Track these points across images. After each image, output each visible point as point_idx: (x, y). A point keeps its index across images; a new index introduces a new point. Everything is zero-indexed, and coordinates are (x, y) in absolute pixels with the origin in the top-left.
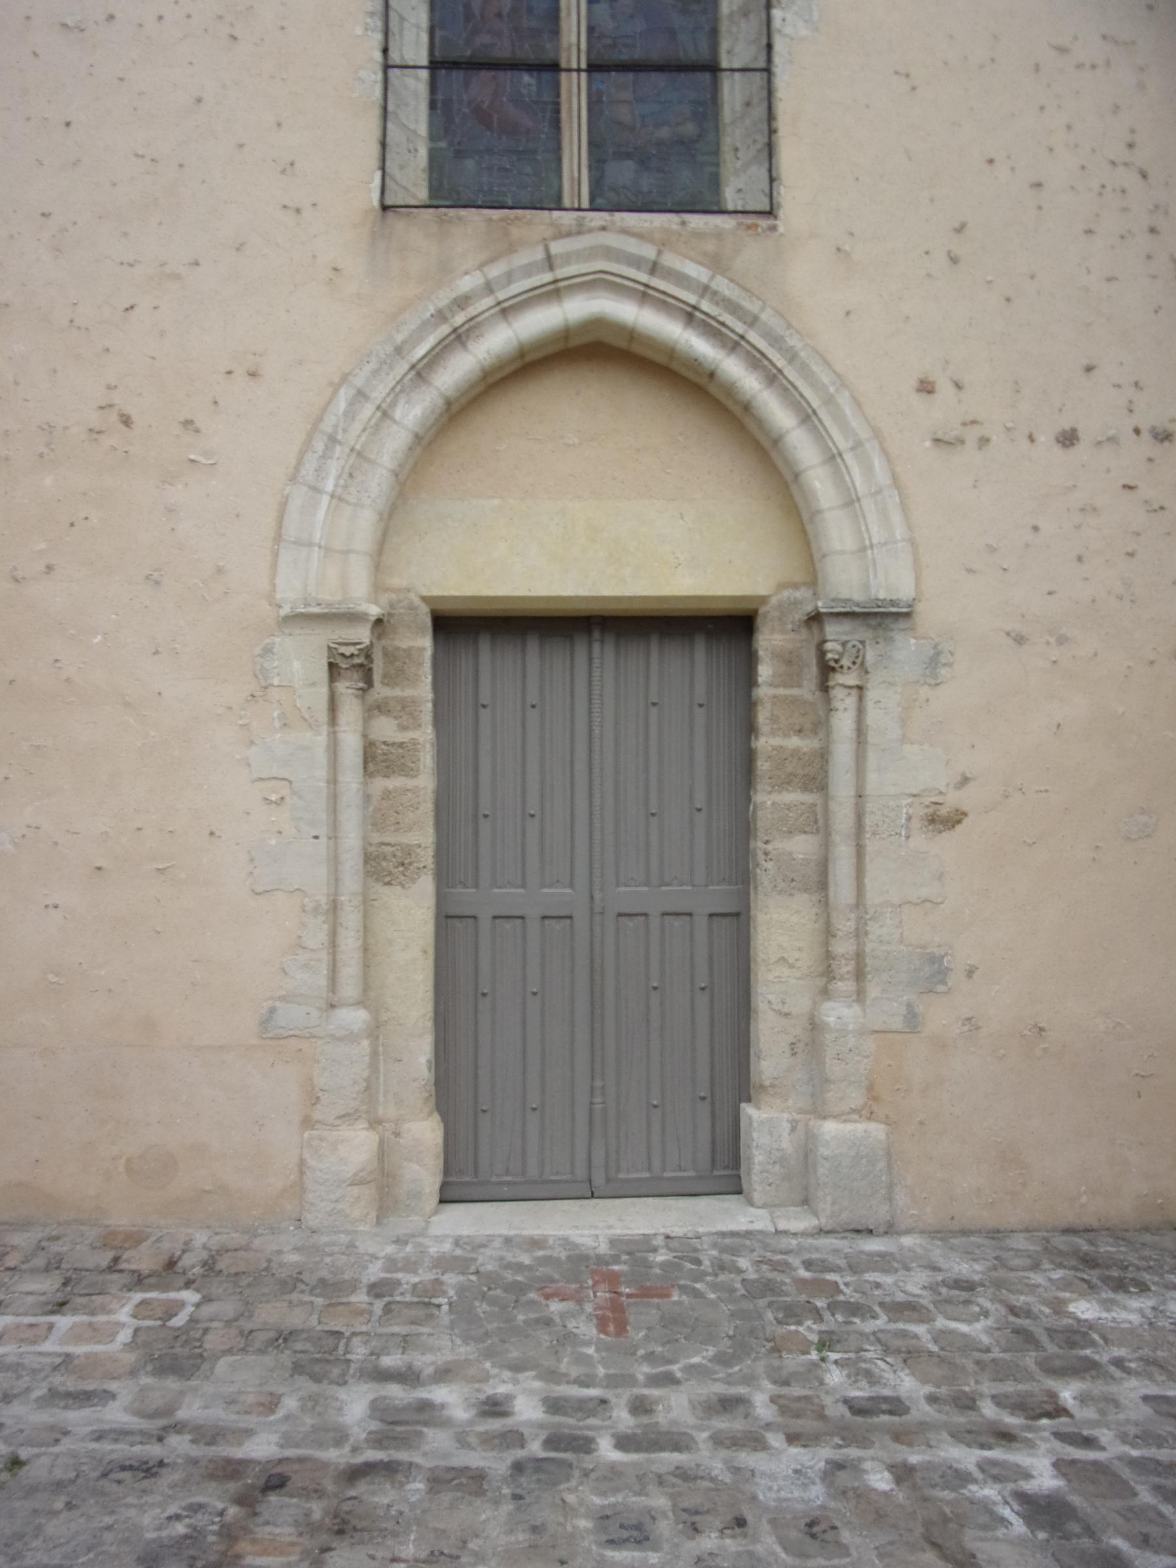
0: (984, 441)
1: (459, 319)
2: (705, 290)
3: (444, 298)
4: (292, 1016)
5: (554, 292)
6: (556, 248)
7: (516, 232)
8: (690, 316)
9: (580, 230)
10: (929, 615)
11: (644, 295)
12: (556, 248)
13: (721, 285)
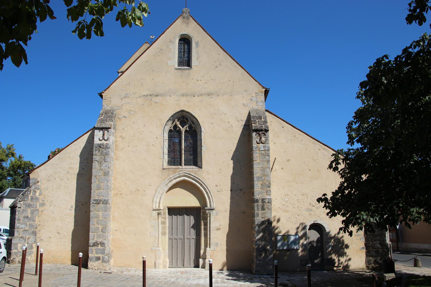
0: (222, 191)
2: (194, 177)
3: (169, 178)
4: (154, 248)
5: (180, 177)
6: (180, 173)
8: (193, 179)
10: (216, 209)
11: (189, 177)
12: (180, 173)
13: (196, 176)
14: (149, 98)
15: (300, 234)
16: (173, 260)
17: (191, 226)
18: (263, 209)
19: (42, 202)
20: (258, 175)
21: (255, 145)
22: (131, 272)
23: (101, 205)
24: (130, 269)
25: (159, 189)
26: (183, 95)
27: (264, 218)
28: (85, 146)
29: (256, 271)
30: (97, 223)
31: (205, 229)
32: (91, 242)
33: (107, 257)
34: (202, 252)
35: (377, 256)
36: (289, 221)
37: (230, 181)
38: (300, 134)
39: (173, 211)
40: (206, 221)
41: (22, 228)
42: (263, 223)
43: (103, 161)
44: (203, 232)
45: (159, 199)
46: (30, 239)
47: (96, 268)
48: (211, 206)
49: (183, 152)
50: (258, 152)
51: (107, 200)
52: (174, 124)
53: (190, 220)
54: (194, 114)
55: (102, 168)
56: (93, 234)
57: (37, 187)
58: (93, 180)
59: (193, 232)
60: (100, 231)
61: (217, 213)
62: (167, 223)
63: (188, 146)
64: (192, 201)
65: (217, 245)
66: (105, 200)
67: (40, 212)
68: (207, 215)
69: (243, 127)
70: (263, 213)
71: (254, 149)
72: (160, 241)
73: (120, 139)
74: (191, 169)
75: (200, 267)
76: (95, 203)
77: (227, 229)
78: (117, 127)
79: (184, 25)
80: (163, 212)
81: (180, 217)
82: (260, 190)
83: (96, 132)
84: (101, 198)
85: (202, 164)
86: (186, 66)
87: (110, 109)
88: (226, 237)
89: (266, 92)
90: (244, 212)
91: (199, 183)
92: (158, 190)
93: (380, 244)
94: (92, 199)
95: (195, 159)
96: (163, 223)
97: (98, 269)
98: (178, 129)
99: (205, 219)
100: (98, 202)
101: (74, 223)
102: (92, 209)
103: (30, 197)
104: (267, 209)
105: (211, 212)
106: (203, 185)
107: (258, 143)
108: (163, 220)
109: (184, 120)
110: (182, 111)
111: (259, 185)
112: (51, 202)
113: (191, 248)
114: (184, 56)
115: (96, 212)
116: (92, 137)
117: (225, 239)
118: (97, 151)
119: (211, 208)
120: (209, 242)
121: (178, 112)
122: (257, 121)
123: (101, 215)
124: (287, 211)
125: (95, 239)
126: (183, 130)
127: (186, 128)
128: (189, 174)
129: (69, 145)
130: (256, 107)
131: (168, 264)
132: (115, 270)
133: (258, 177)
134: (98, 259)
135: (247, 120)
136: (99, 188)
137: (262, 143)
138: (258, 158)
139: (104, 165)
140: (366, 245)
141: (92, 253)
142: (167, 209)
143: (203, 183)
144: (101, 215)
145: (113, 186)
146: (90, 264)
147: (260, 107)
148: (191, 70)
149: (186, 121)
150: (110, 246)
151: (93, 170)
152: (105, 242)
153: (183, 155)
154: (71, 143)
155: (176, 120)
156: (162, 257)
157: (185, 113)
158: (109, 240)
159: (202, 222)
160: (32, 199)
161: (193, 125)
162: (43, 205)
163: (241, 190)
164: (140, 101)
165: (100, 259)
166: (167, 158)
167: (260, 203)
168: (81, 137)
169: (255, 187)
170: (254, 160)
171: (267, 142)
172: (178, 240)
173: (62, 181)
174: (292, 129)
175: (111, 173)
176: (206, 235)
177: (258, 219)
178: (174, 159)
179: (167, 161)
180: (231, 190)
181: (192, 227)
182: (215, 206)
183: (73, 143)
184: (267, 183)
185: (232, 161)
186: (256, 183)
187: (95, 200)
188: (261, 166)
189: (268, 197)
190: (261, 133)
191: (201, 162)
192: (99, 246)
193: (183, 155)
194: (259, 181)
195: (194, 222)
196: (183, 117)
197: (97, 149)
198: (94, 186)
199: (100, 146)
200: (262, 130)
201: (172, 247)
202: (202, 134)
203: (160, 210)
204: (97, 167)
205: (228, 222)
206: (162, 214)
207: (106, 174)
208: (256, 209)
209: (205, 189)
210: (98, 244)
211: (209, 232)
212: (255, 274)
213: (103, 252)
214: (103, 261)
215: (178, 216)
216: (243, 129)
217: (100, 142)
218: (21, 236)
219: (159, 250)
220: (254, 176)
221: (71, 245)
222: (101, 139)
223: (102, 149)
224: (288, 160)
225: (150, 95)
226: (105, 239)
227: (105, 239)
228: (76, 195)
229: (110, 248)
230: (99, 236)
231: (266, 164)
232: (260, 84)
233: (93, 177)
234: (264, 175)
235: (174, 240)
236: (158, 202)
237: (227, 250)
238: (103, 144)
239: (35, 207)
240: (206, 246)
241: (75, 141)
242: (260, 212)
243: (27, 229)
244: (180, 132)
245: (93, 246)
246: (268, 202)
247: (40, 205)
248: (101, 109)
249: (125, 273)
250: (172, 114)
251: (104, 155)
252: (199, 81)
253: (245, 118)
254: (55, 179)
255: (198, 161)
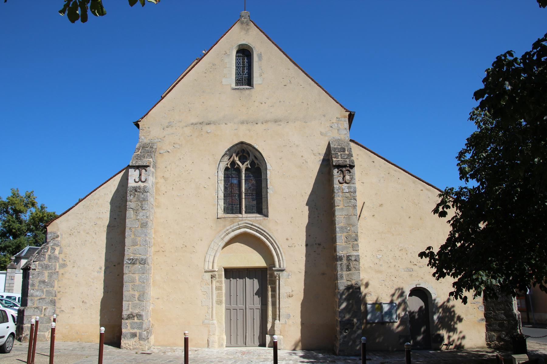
0: (295, 246)
1: (227, 232)
2: (258, 228)
3: (225, 229)
4: (206, 321)
5: (239, 228)
6: (239, 223)
7: (234, 221)
8: (257, 231)
9: (242, 220)
10: (287, 269)
11: (251, 228)
12: (239, 223)
13: (261, 227)
14: (199, 126)
15: (397, 302)
16: (232, 337)
17: (255, 292)
18: (348, 269)
19: (63, 263)
20: (342, 225)
21: (336, 185)
22: (177, 353)
23: (138, 266)
24: (175, 348)
25: (212, 244)
26: (242, 123)
27: (350, 281)
28: (117, 189)
29: (340, 351)
30: (133, 289)
31: (274, 296)
32: (125, 313)
33: (145, 332)
34: (269, 326)
35: (502, 331)
36: (383, 285)
37: (305, 234)
38: (395, 171)
39: (231, 273)
40: (274, 286)
41: (37, 296)
42: (349, 288)
43: (140, 209)
44: (270, 299)
45: (213, 257)
46: (48, 310)
47: (131, 348)
48: (280, 266)
49: (244, 197)
50: (341, 194)
51: (145, 260)
52: (232, 159)
53: (253, 285)
54: (256, 147)
55: (138, 217)
56: (128, 303)
57: (57, 242)
58: (126, 234)
59: (257, 299)
60: (137, 299)
61: (289, 275)
62: (224, 288)
63: (250, 188)
64: (255, 260)
65: (288, 316)
66: (142, 259)
67: (60, 275)
68: (275, 277)
69: (320, 162)
70: (348, 275)
71: (335, 190)
72: (214, 312)
73: (162, 181)
74: (254, 218)
75: (267, 345)
76: (130, 263)
77: (301, 296)
78: (158, 165)
79: (243, 32)
80: (219, 275)
81: (240, 281)
82: (344, 244)
83: (131, 171)
84: (138, 256)
85: (268, 212)
86: (246, 85)
87: (149, 142)
88: (300, 306)
89: (351, 117)
90: (323, 274)
91: (265, 237)
92: (212, 246)
93: (505, 314)
94: (126, 257)
95: (259, 205)
96: (219, 288)
97: (134, 349)
98: (236, 166)
99: (273, 283)
100: (133, 262)
101: (104, 289)
102: (126, 270)
103: (47, 256)
104: (353, 269)
105: (281, 274)
106: (270, 238)
107: (340, 183)
108: (218, 284)
109: (244, 154)
110: (242, 143)
111: (343, 238)
112: (74, 262)
113: (255, 320)
114: (243, 72)
115: (130, 275)
116: (125, 179)
117: (299, 309)
118: (132, 196)
119: (280, 269)
120: (278, 313)
121: (237, 144)
122: (339, 154)
123: (137, 278)
124: (380, 272)
125: (130, 310)
126: (243, 167)
127: (247, 165)
128: (252, 225)
129: (96, 189)
130: (337, 136)
131: (225, 341)
132: (156, 351)
133: (342, 228)
134: (134, 335)
135: (325, 154)
136: (135, 244)
137: (346, 183)
138: (342, 203)
139: (141, 214)
140: (485, 315)
141: (126, 328)
142: (223, 270)
143: (270, 236)
144: (137, 278)
145: (153, 240)
146: (123, 342)
147: (342, 137)
148: (253, 90)
149: (247, 156)
150: (149, 319)
151: (127, 220)
152: (143, 313)
153: (244, 200)
154: (100, 187)
155: (234, 155)
156: (217, 333)
157: (245, 146)
158: (148, 311)
159: (269, 286)
160: (50, 258)
161: (256, 161)
162: (64, 266)
163: (319, 245)
164: (188, 131)
165: (136, 336)
166: (223, 204)
167: (345, 261)
168: (112, 178)
169: (338, 241)
170: (336, 205)
171: (353, 182)
172: (238, 311)
173: (88, 235)
174: (385, 164)
175: (150, 224)
176: (274, 304)
178: (232, 206)
179: (223, 208)
180: (307, 245)
181: (256, 294)
182: (285, 266)
183: (101, 186)
184: (354, 235)
185: (307, 207)
186: (338, 235)
187: (129, 259)
188: (344, 213)
189: (355, 253)
190: (344, 169)
191: (267, 208)
192: (136, 318)
193: (244, 200)
194: (343, 232)
195: (258, 287)
196: (243, 151)
197: (131, 193)
198: (128, 241)
199: (135, 189)
200: (345, 166)
201: (231, 320)
202: (268, 172)
203: (215, 271)
204: (132, 216)
205: (303, 287)
206: (217, 276)
207: (144, 225)
208: (339, 269)
209: (272, 244)
210: (134, 317)
211: (278, 300)
212: (339, 355)
213: (140, 326)
214: (141, 339)
215: (238, 279)
216: (321, 165)
217: (135, 185)
218: (35, 306)
219: (214, 324)
220: (337, 225)
221: (99, 318)
222: (137, 180)
223: (138, 194)
224: (381, 205)
225: (200, 123)
226: (143, 310)
227: (143, 309)
228: (106, 253)
229: (150, 322)
230: (135, 306)
231: (352, 210)
232: (342, 106)
233: (127, 230)
234: (349, 225)
235: (232, 311)
236: (212, 261)
237: (302, 324)
238: (139, 187)
239: (53, 268)
240: (274, 319)
241: (104, 183)
242: (345, 273)
243: (44, 297)
244: (239, 170)
245: (127, 319)
246: (356, 260)
247: (60, 267)
248: (137, 141)
249: (169, 354)
250: (229, 147)
251: (141, 202)
252: (264, 103)
253: (323, 151)
254: (79, 232)
255: (263, 207)
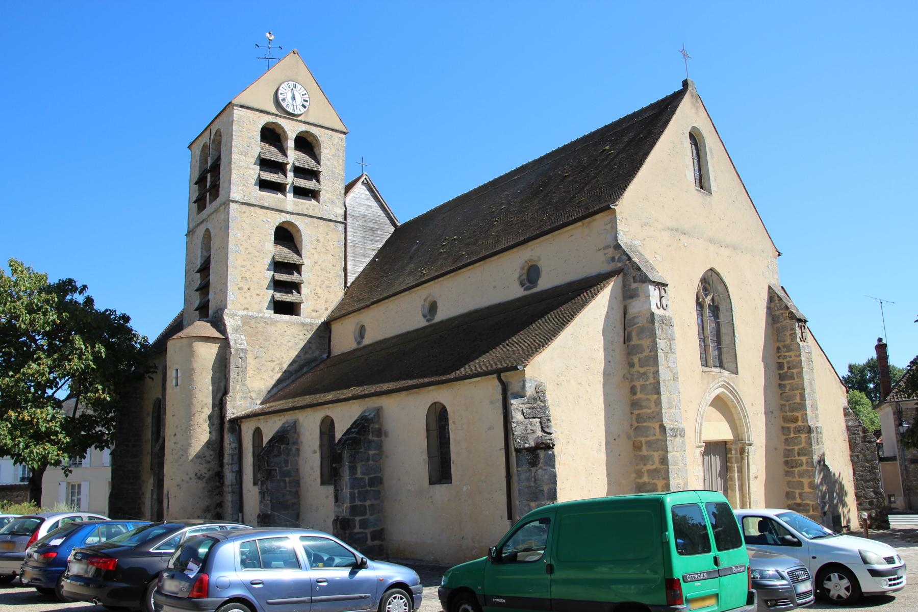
42: (819, 462)
58: (662, 389)
90: (776, 449)
161: (716, 298)
177: (816, 458)
187: (672, 430)
251: (670, 340)
253: (765, 296)
